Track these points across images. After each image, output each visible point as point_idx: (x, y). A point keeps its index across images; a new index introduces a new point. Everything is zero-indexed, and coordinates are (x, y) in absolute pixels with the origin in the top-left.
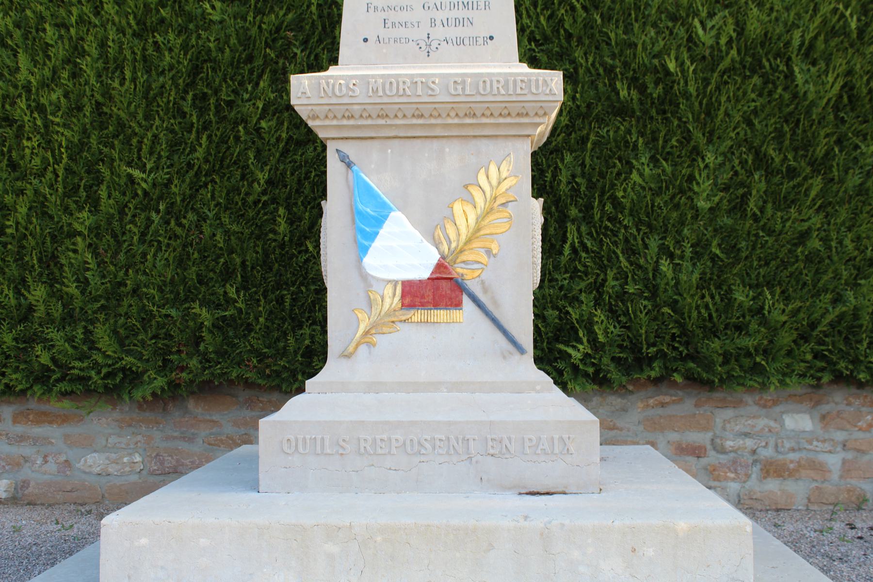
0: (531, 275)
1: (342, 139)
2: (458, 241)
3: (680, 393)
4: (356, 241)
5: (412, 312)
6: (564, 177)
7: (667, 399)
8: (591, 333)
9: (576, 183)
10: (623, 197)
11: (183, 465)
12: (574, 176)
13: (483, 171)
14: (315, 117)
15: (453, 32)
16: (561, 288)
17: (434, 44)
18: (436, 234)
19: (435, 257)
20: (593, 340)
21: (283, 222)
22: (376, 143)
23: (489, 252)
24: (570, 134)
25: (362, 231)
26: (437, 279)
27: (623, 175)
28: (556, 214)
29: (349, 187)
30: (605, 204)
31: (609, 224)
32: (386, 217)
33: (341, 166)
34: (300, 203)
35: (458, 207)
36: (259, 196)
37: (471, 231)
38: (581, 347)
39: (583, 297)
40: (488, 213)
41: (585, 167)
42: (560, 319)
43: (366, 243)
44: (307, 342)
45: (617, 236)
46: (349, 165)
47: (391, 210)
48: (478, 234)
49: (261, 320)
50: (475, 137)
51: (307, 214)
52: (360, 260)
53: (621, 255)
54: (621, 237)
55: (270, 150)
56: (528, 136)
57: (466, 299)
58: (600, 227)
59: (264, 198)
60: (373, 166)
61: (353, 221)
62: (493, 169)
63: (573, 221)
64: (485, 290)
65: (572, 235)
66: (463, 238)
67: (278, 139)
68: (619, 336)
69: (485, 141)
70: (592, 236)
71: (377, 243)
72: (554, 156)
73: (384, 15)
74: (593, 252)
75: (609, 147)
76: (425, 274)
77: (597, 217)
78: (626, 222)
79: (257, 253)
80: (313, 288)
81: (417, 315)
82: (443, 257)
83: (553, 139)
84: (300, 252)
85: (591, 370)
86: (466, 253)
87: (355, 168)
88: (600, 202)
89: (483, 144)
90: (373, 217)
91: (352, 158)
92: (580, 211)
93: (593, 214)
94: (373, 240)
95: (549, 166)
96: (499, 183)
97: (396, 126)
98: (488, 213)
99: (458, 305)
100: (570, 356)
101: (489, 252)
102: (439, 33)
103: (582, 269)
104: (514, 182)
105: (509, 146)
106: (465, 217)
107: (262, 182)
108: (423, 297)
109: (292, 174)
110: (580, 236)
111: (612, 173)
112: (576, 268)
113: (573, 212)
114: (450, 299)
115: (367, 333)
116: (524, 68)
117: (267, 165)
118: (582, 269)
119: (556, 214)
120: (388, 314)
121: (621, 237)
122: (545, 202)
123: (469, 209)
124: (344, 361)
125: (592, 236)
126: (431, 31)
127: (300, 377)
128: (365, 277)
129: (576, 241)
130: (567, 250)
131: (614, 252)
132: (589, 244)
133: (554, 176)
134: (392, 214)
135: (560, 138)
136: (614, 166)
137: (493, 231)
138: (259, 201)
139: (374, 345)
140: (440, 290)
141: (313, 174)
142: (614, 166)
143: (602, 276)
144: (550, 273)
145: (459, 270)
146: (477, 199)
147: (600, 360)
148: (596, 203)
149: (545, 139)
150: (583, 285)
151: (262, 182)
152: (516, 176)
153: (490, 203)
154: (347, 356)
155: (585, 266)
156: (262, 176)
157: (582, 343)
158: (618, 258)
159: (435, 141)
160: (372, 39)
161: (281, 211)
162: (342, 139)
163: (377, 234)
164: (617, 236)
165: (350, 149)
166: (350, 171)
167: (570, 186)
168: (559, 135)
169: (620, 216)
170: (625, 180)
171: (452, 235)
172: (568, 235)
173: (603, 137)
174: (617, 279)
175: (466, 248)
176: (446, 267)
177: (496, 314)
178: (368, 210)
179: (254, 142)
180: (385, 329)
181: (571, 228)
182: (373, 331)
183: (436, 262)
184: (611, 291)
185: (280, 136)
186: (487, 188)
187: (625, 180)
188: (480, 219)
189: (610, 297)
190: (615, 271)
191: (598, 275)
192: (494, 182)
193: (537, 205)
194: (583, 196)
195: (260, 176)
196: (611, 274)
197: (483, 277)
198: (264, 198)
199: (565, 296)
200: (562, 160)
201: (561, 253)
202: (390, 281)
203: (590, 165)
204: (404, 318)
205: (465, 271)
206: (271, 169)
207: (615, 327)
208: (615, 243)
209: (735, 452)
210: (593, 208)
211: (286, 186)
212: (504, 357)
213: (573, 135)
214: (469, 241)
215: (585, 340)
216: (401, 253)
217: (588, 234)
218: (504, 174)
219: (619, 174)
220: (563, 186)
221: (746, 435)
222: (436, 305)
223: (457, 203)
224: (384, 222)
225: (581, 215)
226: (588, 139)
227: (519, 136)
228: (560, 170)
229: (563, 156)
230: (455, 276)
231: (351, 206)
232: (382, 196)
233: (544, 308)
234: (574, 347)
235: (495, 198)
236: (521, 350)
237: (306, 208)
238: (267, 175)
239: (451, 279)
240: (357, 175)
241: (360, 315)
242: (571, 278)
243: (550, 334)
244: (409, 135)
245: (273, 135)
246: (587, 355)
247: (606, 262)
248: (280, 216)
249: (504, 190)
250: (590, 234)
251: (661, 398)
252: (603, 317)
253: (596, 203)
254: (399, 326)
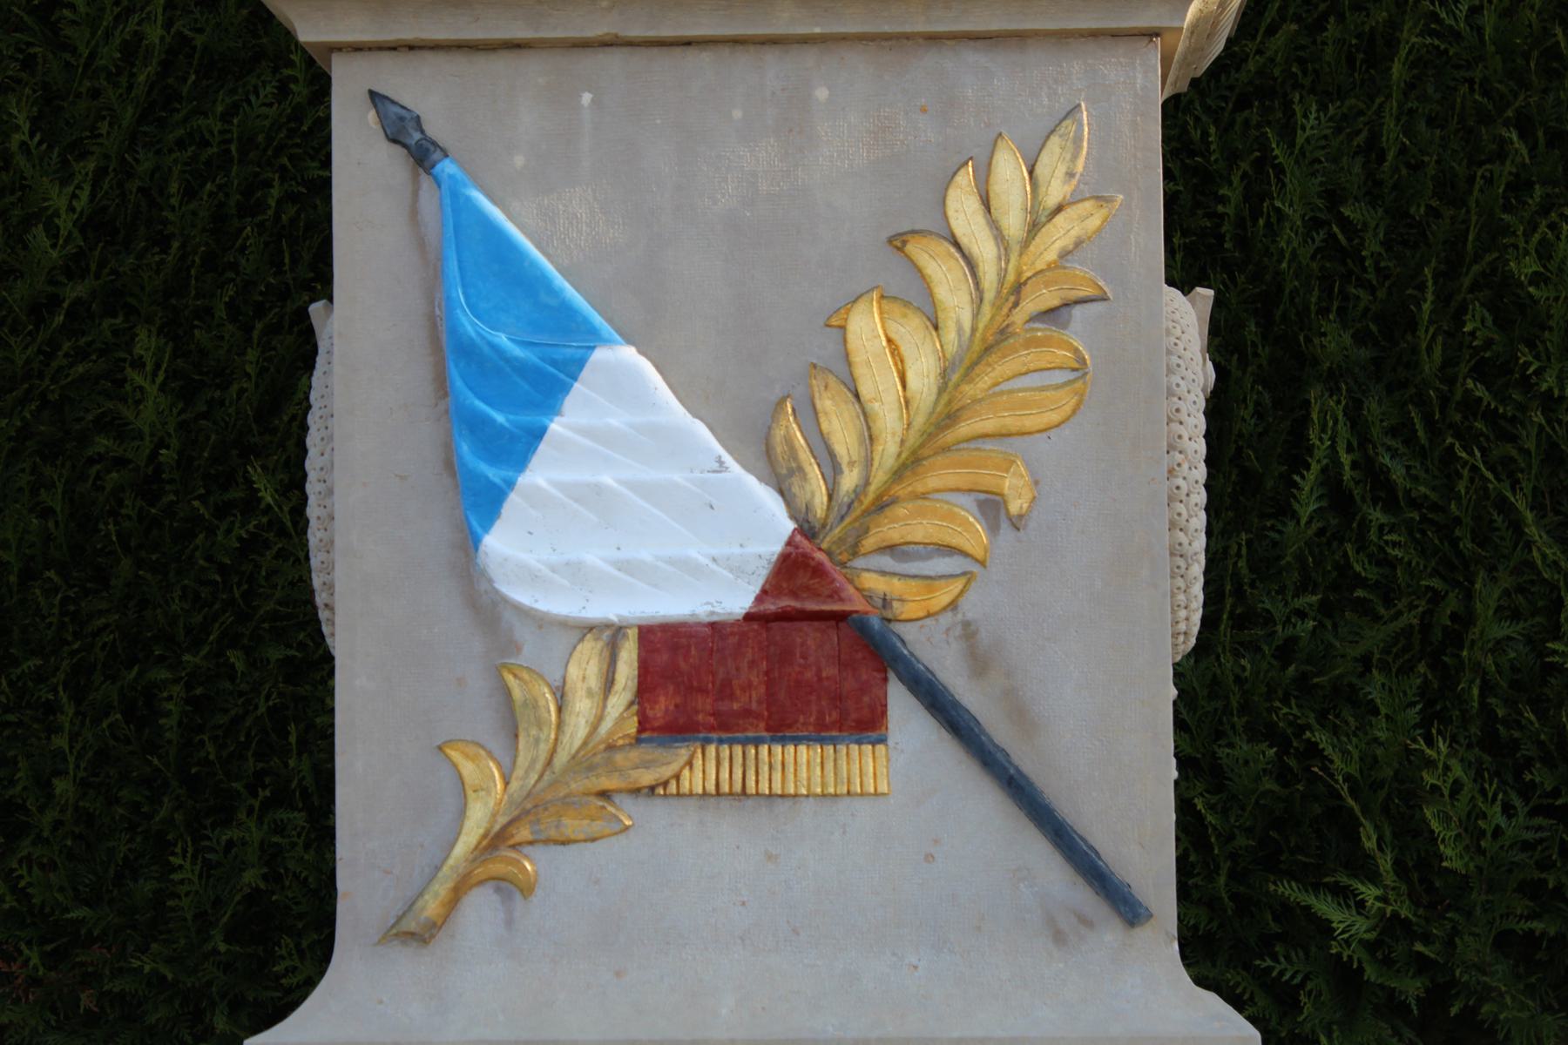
0: (1170, 602)
1: (393, 48)
2: (868, 462)
4: (450, 464)
5: (683, 753)
6: (1292, 202)
8: (1409, 833)
9: (1345, 223)
10: (1536, 279)
12: (1334, 197)
13: (966, 177)
16: (1286, 652)
18: (779, 434)
19: (773, 527)
20: (1420, 868)
21: (152, 390)
22: (533, 68)
23: (992, 506)
24: (1319, 25)
25: (477, 426)
26: (785, 616)
27: (1538, 191)
28: (1264, 352)
29: (421, 244)
30: (1463, 309)
31: (1480, 391)
32: (573, 368)
33: (388, 161)
34: (221, 312)
35: (866, 328)
36: (52, 282)
37: (919, 421)
38: (1369, 893)
39: (1375, 688)
40: (988, 350)
41: (1381, 158)
42: (1283, 775)
43: (493, 474)
44: (251, 877)
45: (1513, 439)
47: (593, 338)
48: (950, 436)
49: (62, 787)
50: (933, 39)
51: (252, 355)
52: (470, 544)
53: (1529, 516)
54: (1531, 445)
55: (95, 94)
56: (1151, 34)
57: (900, 702)
58: (1445, 400)
59: (75, 291)
60: (519, 161)
61: (442, 386)
62: (1008, 170)
63: (1332, 380)
64: (979, 662)
65: (1329, 438)
66: (888, 451)
67: (132, 50)
68: (1526, 846)
69: (974, 57)
70: (1410, 440)
71: (538, 476)
72: (1253, 114)
74: (1414, 503)
75: (1478, 74)
76: (734, 599)
77: (1430, 364)
78: (1549, 381)
79: (46, 513)
80: (275, 654)
81: (703, 766)
82: (807, 529)
83: (1251, 47)
84: (222, 511)
85: (1412, 988)
86: (900, 511)
87: (447, 168)
88: (1443, 299)
89: (970, 73)
90: (521, 368)
91: (436, 128)
92: (1361, 338)
93: (1414, 350)
94: (521, 463)
95: (1233, 157)
96: (1034, 228)
98: (988, 350)
99: (867, 724)
100: (1325, 928)
101: (992, 506)
103: (1371, 573)
104: (1095, 222)
105: (1075, 72)
106: (894, 364)
107: (65, 223)
108: (725, 690)
109: (189, 193)
110: (1362, 440)
111: (1489, 181)
112: (1344, 568)
113: (1334, 341)
114: (837, 698)
115: (495, 841)
117: (83, 156)
118: (1371, 573)
119: (1264, 352)
120: (583, 762)
121: (1531, 445)
122: (1218, 303)
123: (910, 331)
124: (405, 960)
125: (1410, 440)
127: (221, 1023)
128: (488, 612)
129: (1346, 459)
130: (1308, 499)
131: (1503, 505)
132: (1398, 473)
133: (1255, 197)
134: (600, 355)
135: (1278, 42)
136: (1501, 155)
137: (1010, 422)
138: (54, 301)
139: (526, 889)
140: (790, 666)
141: (275, 192)
142: (1501, 155)
143: (1452, 603)
144: (1239, 592)
145: (873, 579)
146: (941, 292)
147: (1450, 944)
148: (1426, 307)
149: (1218, 47)
150: (1374, 638)
151: (65, 223)
152: (1100, 199)
153: (997, 307)
154: (413, 933)
155: (1385, 562)
156: (66, 203)
157: (1373, 877)
158: (1517, 526)
159: (771, 57)
161: (146, 343)
162: (393, 48)
163: (537, 434)
164: (1513, 439)
165: (425, 91)
166: (426, 181)
167: (1320, 236)
168: (1272, 31)
169: (1525, 356)
170: (1545, 210)
171: (842, 434)
172: (1313, 436)
173: (1457, 36)
174: (1516, 616)
175: (900, 490)
176: (818, 571)
177: (1025, 760)
178: (502, 340)
179: (28, 63)
180: (572, 825)
181: (1325, 408)
182: (524, 833)
183: (776, 548)
184: (1489, 662)
185: (139, 36)
186: (984, 249)
187: (1545, 210)
188: (956, 372)
189: (1487, 688)
190: (1506, 582)
191: (1436, 598)
192: (1014, 223)
193: (1187, 316)
194: (1371, 276)
195: (58, 199)
196: (1488, 594)
197: (972, 608)
198: (75, 291)
199: (1302, 680)
200: (1288, 131)
201: (1283, 509)
202: (589, 629)
203: (1403, 150)
204: (647, 778)
205: (896, 586)
206: (101, 172)
207: (1508, 810)
208: (1505, 469)
210: (1412, 326)
211: (163, 242)
212: (1059, 938)
213: (1332, 30)
214: (910, 464)
215: (1385, 863)
216: (634, 511)
217: (1393, 432)
218: (1055, 191)
219: (1520, 186)
220: (1289, 239)
222: (781, 724)
223: (861, 306)
224: (565, 389)
225: (1364, 354)
226: (1392, 44)
227: (1116, 34)
228: (1280, 171)
229: (1289, 114)
230: (858, 605)
231: (433, 323)
232: (559, 281)
233: (1219, 734)
234: (1342, 894)
235: (1018, 288)
236: (1126, 906)
237: (248, 329)
238: (85, 195)
239: (840, 617)
240: (455, 195)
241: (468, 769)
242: (1325, 608)
243: (1242, 841)
244: (666, 32)
245: (108, 35)
246: (1392, 926)
247: (1467, 545)
248: (139, 364)
249: (1051, 255)
250: (1402, 430)
252: (1458, 771)
253: (1426, 307)
254: (628, 811)
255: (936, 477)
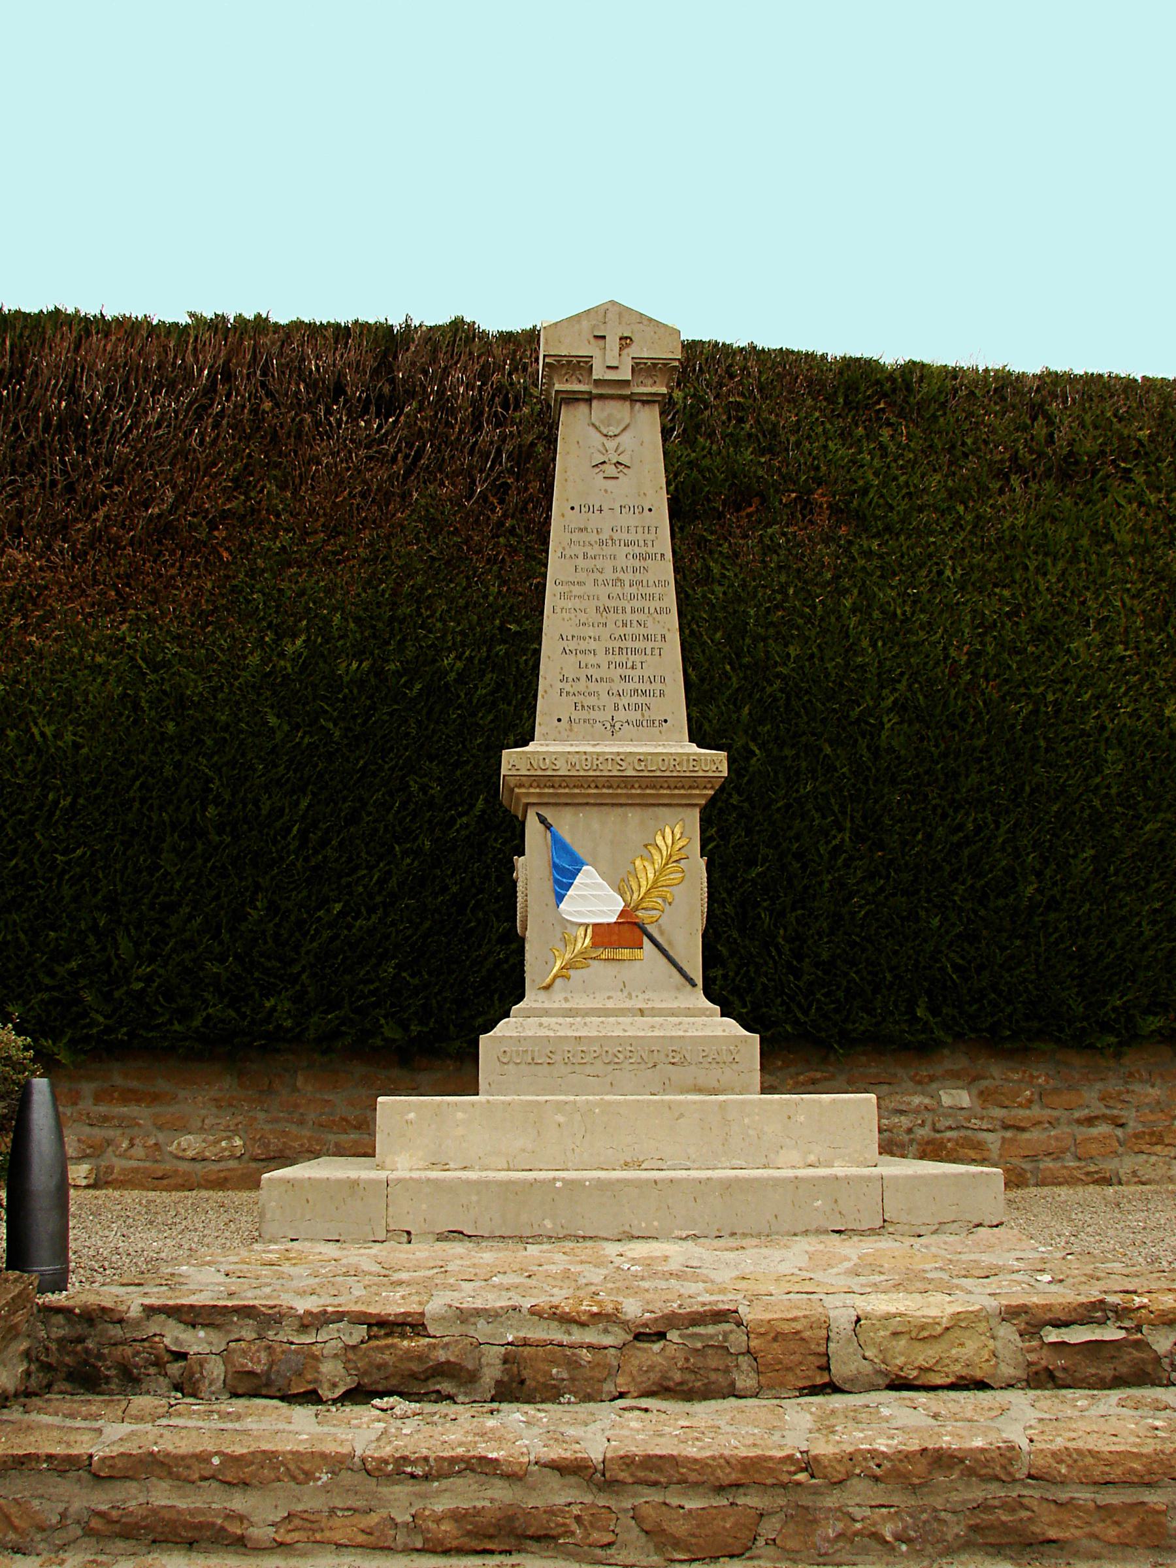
3: (831, 1069)
7: (818, 1075)
11: (291, 1148)
14: (521, 786)
15: (635, 716)
17: (618, 726)
19: (621, 905)
46: (548, 827)
47: (583, 864)
62: (668, 830)
64: (662, 933)
66: (643, 890)
69: (664, 809)
73: (576, 699)
97: (589, 795)
102: (621, 715)
116: (694, 748)
126: (615, 714)
140: (627, 932)
160: (565, 719)
165: (546, 813)
177: (671, 953)
186: (664, 849)
192: (669, 842)
193: (702, 863)
209: (890, 1131)
216: (593, 900)
221: (902, 1112)
251: (811, 1074)
255: (655, 892)
